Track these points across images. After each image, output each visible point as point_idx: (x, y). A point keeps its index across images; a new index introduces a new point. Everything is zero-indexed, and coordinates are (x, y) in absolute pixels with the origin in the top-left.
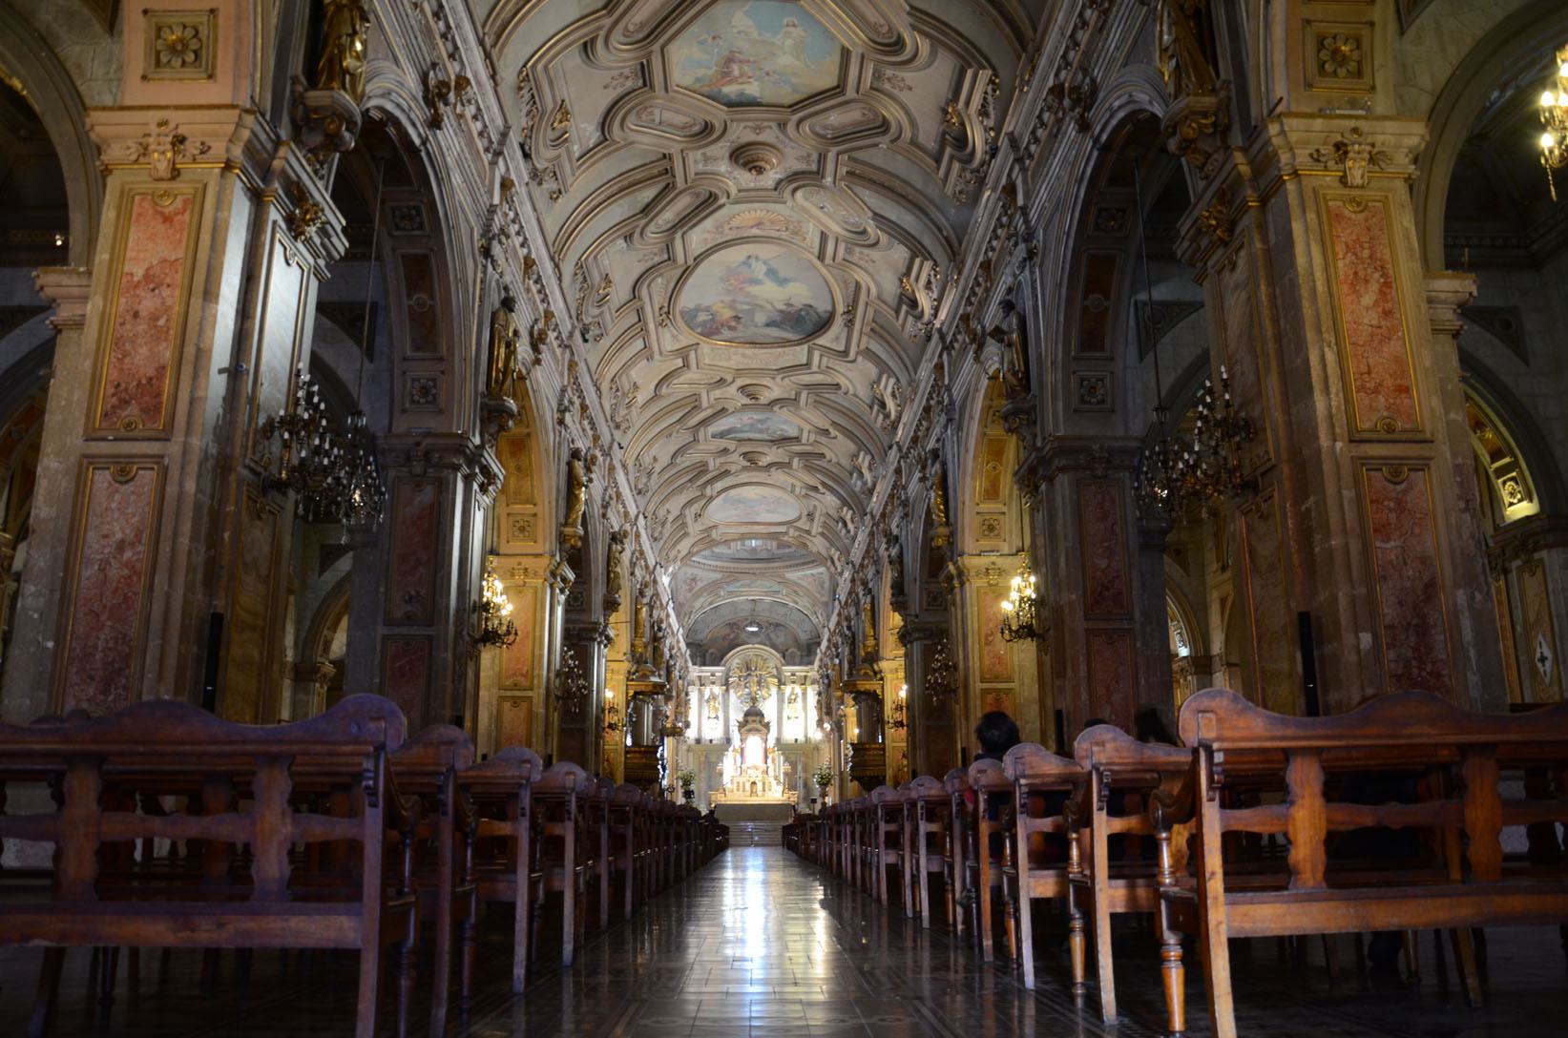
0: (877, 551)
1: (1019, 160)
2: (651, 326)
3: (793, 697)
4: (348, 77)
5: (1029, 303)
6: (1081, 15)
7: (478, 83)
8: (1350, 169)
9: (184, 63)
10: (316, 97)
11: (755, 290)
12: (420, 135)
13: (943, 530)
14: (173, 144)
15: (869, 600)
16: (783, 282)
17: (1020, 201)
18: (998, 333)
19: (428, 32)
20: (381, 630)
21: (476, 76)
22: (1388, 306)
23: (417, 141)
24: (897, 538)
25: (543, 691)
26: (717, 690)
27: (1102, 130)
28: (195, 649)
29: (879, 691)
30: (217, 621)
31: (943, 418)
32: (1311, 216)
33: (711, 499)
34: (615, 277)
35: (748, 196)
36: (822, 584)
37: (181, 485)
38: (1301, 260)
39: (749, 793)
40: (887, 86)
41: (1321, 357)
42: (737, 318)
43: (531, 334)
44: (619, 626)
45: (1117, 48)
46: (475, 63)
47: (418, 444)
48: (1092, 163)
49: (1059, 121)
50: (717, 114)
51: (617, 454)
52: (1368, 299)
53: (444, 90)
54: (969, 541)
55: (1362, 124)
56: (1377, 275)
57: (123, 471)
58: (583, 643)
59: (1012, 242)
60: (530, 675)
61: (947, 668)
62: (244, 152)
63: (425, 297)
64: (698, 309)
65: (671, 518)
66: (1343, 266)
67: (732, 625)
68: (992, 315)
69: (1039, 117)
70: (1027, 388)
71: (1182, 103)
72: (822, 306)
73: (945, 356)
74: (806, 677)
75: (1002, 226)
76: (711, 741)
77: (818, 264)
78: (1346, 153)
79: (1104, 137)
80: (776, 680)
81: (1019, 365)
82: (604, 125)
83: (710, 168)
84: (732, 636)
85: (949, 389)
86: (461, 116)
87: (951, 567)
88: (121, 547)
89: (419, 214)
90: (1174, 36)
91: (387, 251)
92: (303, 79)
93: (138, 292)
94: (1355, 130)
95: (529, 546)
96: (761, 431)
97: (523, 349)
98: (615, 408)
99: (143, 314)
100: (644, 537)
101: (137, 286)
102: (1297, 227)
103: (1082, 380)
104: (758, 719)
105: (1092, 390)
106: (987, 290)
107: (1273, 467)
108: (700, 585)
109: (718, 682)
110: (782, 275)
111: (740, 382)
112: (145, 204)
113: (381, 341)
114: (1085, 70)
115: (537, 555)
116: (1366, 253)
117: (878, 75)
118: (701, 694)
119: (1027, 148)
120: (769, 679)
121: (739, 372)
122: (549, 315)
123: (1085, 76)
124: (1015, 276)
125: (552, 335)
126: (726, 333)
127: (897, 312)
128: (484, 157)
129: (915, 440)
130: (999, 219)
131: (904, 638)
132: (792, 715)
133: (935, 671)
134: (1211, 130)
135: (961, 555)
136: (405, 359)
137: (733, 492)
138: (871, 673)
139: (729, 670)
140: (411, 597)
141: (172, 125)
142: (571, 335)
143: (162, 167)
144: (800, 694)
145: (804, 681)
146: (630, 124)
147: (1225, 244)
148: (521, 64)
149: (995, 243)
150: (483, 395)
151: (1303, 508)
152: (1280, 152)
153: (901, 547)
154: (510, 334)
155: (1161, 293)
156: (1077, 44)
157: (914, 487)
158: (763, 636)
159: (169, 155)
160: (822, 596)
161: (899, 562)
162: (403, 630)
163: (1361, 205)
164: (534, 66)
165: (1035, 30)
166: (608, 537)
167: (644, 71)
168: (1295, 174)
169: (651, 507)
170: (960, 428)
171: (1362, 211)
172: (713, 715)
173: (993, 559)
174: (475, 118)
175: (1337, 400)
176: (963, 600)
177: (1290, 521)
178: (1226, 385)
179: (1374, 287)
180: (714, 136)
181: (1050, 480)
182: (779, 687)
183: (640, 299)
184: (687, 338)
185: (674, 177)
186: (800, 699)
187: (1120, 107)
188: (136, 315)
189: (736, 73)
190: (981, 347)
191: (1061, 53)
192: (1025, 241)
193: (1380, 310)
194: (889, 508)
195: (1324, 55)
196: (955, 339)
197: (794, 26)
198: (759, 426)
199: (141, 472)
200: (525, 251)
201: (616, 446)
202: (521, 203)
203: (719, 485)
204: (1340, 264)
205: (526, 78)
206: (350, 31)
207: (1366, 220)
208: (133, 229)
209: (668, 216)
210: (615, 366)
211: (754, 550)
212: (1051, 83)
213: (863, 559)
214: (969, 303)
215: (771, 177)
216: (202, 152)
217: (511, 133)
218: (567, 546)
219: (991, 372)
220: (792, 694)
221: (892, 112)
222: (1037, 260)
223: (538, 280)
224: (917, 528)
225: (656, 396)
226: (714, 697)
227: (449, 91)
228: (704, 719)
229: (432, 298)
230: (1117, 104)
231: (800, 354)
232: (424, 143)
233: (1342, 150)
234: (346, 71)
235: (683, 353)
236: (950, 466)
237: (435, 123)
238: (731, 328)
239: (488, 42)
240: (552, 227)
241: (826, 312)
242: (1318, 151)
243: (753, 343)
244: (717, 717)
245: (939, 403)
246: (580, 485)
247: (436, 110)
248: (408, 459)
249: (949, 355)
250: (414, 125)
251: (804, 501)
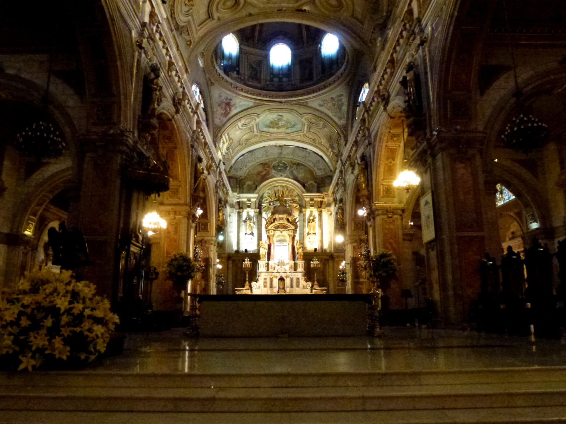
3: (312, 218)
26: (252, 212)
67: (264, 165)
74: (321, 202)
84: (264, 173)
104: (284, 216)
108: (234, 111)
109: (253, 206)
132: (312, 232)
139: (262, 197)
144: (317, 216)
145: (320, 205)
158: (287, 172)
160: (340, 118)
182: (301, 212)
186: (317, 220)
220: (311, 215)
226: (249, 218)
244: (252, 234)
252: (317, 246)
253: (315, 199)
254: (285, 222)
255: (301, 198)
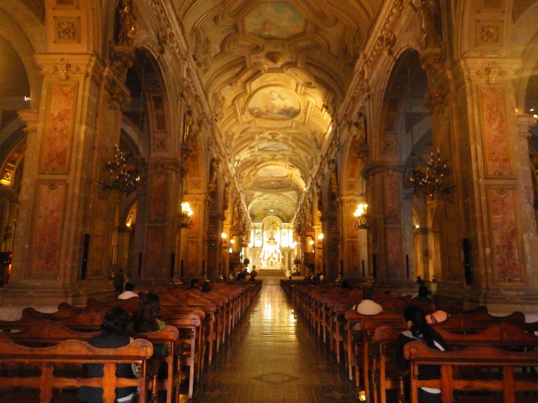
0: (313, 189)
1: (366, 62)
2: (239, 114)
4: (130, 41)
5: (368, 114)
6: (391, 11)
7: (177, 35)
8: (491, 78)
9: (69, 37)
10: (118, 48)
11: (273, 102)
12: (157, 56)
13: (335, 187)
14: (66, 67)
15: (310, 205)
16: (283, 99)
17: (366, 77)
18: (357, 124)
19: (159, 18)
20: (147, 225)
21: (176, 32)
22: (502, 129)
23: (156, 58)
24: (320, 187)
25: (202, 239)
26: (260, 231)
27: (397, 54)
28: (79, 246)
29: (313, 236)
30: (87, 237)
31: (336, 149)
32: (475, 96)
33: (259, 169)
34: (227, 98)
35: (271, 70)
36: (295, 196)
37: (73, 190)
38: (470, 112)
39: (270, 265)
40: (320, 32)
41: (476, 148)
42: (268, 111)
43: (198, 121)
44: (228, 214)
45: (404, 24)
46: (176, 29)
47: (159, 162)
48: (393, 66)
49: (381, 50)
50: (261, 42)
51: (228, 157)
52: (495, 126)
53: (165, 39)
54: (344, 191)
55: (496, 60)
56: (498, 117)
57: (52, 185)
58: (216, 220)
59: (362, 92)
60: (197, 234)
61: (336, 233)
62: (92, 71)
63: (161, 111)
64: (254, 108)
65: (245, 176)
66: (486, 114)
67: (265, 209)
68: (354, 117)
69: (374, 47)
70: (366, 143)
71: (428, 50)
72: (297, 107)
73: (338, 128)
75: (359, 85)
76: (258, 247)
77: (295, 94)
78: (490, 71)
79: (398, 57)
80: (279, 228)
81: (364, 135)
82: (222, 46)
83: (259, 60)
84: (265, 213)
85: (339, 139)
86: (172, 47)
87: (338, 200)
88: (52, 212)
89: (158, 82)
90: (426, 25)
91: (147, 95)
92: (113, 42)
93: (56, 121)
94: (494, 63)
95: (198, 191)
96: (275, 148)
97: (195, 127)
98: (226, 141)
99: (58, 129)
100: (236, 182)
101: (55, 119)
102: (469, 100)
103: (386, 141)
105: (388, 145)
106: (353, 107)
107: (455, 186)
109: (260, 228)
110: (283, 97)
111: (269, 132)
112: (58, 89)
113: (145, 126)
114: (392, 32)
115: (200, 194)
116: (495, 109)
117: (317, 28)
118: (255, 232)
119: (369, 58)
120: (277, 227)
121: (268, 129)
122: (204, 113)
123: (391, 34)
124: (363, 104)
125: (205, 120)
126: (264, 116)
127: (322, 110)
128: (180, 61)
129: (327, 154)
130: (358, 82)
131: (322, 219)
133: (332, 233)
134: (438, 61)
135: (342, 195)
136: (154, 132)
137: (266, 167)
138: (311, 229)
140: (157, 214)
141: (66, 60)
142: (212, 119)
143: (63, 76)
145: (288, 228)
146: (232, 46)
147: (441, 103)
148: (193, 24)
149: (356, 91)
150: (181, 144)
151: (466, 201)
152: (464, 71)
153: (321, 190)
154: (191, 123)
155: (415, 110)
156: (389, 21)
157: (326, 170)
159: (65, 71)
161: (320, 194)
162: (154, 224)
163: (494, 90)
164: (197, 26)
165: (374, 14)
166: (224, 185)
167: (236, 28)
168: (469, 79)
169: (239, 172)
170: (342, 152)
171: (495, 92)
172: (259, 239)
173: (353, 197)
174: (177, 47)
175: (480, 164)
176: (342, 210)
177: (460, 205)
178: (439, 155)
179: (497, 122)
180: (259, 50)
181: (373, 175)
183: (235, 105)
184: (250, 118)
185: (246, 64)
187: (404, 47)
188: (55, 129)
189: (268, 27)
190: (350, 127)
191: (383, 24)
192: (368, 91)
193: (499, 130)
194: (318, 175)
195: (484, 34)
196: (341, 122)
197: (288, 11)
198: (275, 146)
199: (59, 186)
200: (195, 92)
201: (227, 155)
202: (194, 76)
203: (261, 165)
204: (485, 113)
205: (194, 29)
206: (129, 23)
207: (496, 96)
208: (53, 98)
209: (244, 77)
210: (227, 127)
211: (272, 185)
212: (379, 35)
213: (309, 191)
214: (347, 110)
215: (279, 64)
216: (77, 70)
217: (190, 52)
218: (210, 191)
219: (354, 135)
221: (321, 42)
222: (371, 98)
223: (200, 102)
224: (326, 183)
225: (240, 137)
226: (259, 233)
227: (167, 39)
228: (256, 240)
229: (163, 111)
230: (403, 45)
231: (289, 123)
232: (159, 58)
233: (488, 70)
234: (129, 38)
235: (249, 122)
236: (339, 166)
237: (162, 52)
238: (266, 115)
239: (181, 17)
240: (204, 81)
241: (298, 109)
242: (479, 71)
243: (272, 119)
245: (335, 143)
246: (215, 170)
247: (162, 46)
248: (156, 167)
249: (339, 127)
250: (155, 52)
251: (289, 171)
252: (287, 246)
253: (287, 226)
254: (273, 243)
255: (281, 225)
